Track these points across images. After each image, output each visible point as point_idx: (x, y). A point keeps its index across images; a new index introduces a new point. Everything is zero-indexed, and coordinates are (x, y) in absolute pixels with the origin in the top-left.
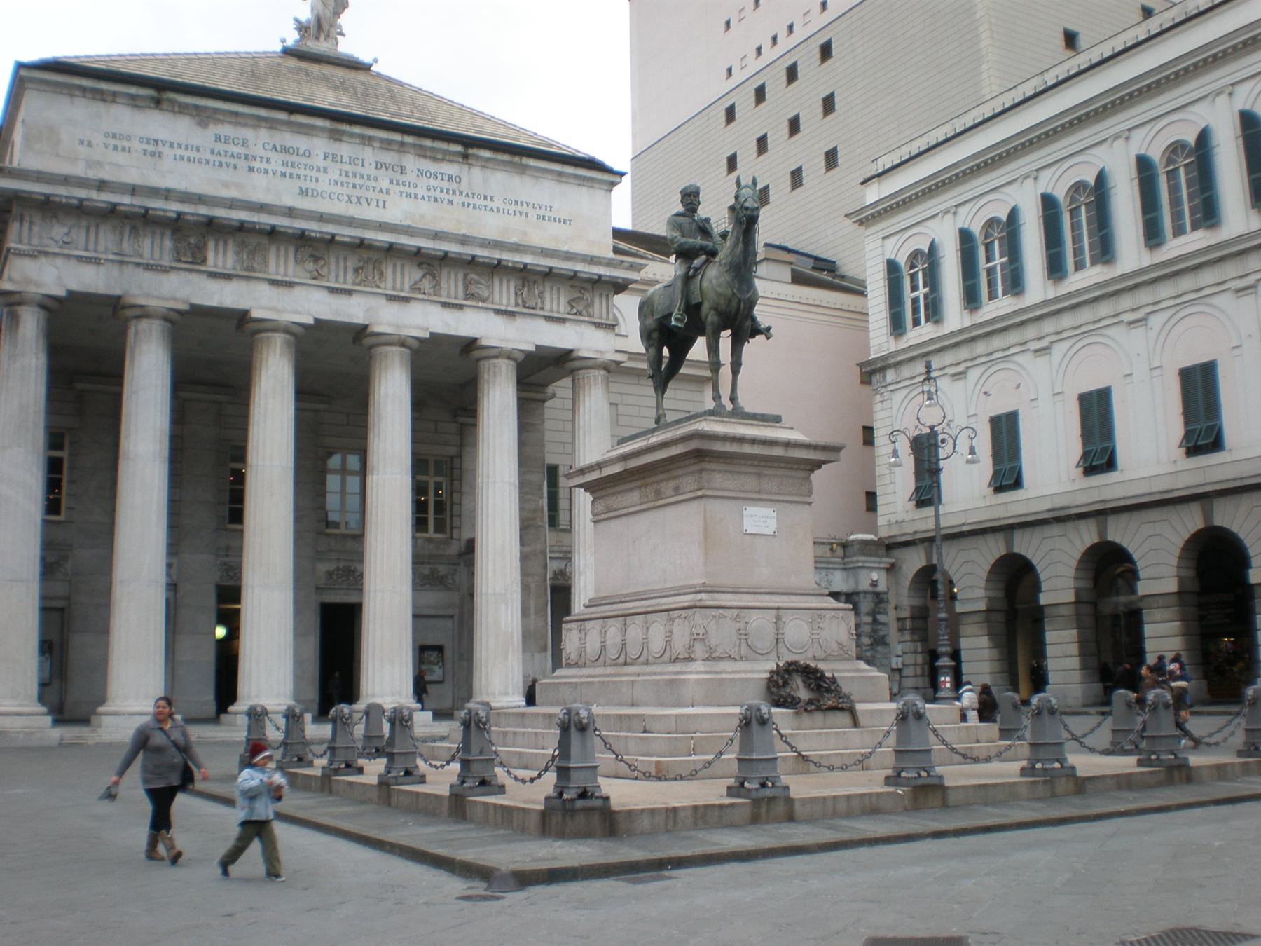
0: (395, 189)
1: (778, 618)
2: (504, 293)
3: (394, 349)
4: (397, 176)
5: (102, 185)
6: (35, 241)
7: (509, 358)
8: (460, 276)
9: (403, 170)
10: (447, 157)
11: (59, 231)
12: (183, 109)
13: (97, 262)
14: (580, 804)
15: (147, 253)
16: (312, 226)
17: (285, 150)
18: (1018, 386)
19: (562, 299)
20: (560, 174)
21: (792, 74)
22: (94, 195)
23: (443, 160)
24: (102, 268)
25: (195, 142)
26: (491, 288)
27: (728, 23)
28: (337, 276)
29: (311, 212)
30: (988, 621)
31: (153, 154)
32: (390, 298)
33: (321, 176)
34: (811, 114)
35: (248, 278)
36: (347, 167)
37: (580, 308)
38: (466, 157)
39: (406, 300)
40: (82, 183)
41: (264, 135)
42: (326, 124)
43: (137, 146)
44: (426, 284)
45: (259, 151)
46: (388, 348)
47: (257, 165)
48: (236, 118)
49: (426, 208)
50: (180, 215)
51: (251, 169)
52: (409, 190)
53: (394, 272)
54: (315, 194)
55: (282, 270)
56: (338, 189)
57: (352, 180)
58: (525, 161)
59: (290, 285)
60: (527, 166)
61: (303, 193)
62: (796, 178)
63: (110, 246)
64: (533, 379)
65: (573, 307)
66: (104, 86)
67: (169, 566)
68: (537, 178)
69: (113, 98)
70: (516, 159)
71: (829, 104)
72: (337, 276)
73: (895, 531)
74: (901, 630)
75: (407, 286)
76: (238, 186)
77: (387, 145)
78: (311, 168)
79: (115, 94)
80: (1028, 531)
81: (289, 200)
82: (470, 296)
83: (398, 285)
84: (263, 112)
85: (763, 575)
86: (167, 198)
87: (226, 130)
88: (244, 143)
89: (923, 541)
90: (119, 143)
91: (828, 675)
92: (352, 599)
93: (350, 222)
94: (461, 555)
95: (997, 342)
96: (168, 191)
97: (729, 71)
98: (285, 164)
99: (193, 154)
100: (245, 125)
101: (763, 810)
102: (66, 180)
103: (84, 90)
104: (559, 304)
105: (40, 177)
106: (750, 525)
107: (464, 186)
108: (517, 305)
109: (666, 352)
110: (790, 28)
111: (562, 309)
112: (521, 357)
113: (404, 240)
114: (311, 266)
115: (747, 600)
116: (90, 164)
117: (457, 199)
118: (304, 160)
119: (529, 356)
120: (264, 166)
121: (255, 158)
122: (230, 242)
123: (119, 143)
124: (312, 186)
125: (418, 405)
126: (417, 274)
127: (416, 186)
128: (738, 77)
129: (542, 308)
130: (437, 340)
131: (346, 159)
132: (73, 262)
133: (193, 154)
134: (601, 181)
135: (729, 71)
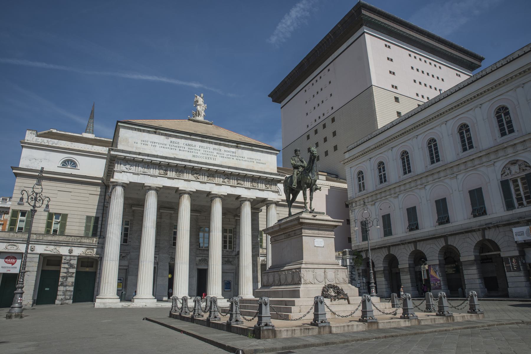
0: (218, 155)
2: (248, 184)
5: (140, 154)
7: (249, 201)
10: (232, 146)
11: (128, 166)
12: (162, 134)
14: (265, 328)
15: (152, 172)
17: (189, 145)
21: (324, 126)
25: (165, 143)
27: (307, 114)
30: (384, 273)
31: (154, 146)
32: (217, 184)
33: (198, 152)
34: (330, 136)
36: (205, 150)
39: (221, 185)
41: (183, 141)
43: (149, 143)
44: (226, 180)
45: (182, 145)
47: (181, 149)
49: (226, 160)
50: (160, 162)
51: (180, 150)
54: (196, 157)
56: (203, 155)
59: (189, 181)
62: (326, 153)
64: (256, 207)
67: (155, 257)
69: (144, 131)
71: (334, 134)
73: (357, 248)
74: (359, 276)
76: (176, 154)
79: (144, 130)
80: (394, 247)
81: (189, 158)
85: (321, 259)
87: (174, 139)
88: (178, 143)
89: (364, 251)
91: (340, 288)
92: (206, 268)
94: (236, 255)
95: (383, 195)
96: (157, 155)
97: (308, 126)
98: (189, 149)
99: (165, 146)
101: (322, 330)
102: (130, 152)
105: (123, 151)
109: (291, 195)
110: (324, 115)
112: (252, 200)
114: (195, 175)
115: (316, 266)
116: (137, 148)
117: (235, 158)
118: (194, 148)
119: (254, 200)
120: (183, 149)
123: (145, 143)
124: (196, 154)
125: (224, 214)
128: (310, 127)
130: (229, 195)
133: (165, 146)
135: (308, 126)
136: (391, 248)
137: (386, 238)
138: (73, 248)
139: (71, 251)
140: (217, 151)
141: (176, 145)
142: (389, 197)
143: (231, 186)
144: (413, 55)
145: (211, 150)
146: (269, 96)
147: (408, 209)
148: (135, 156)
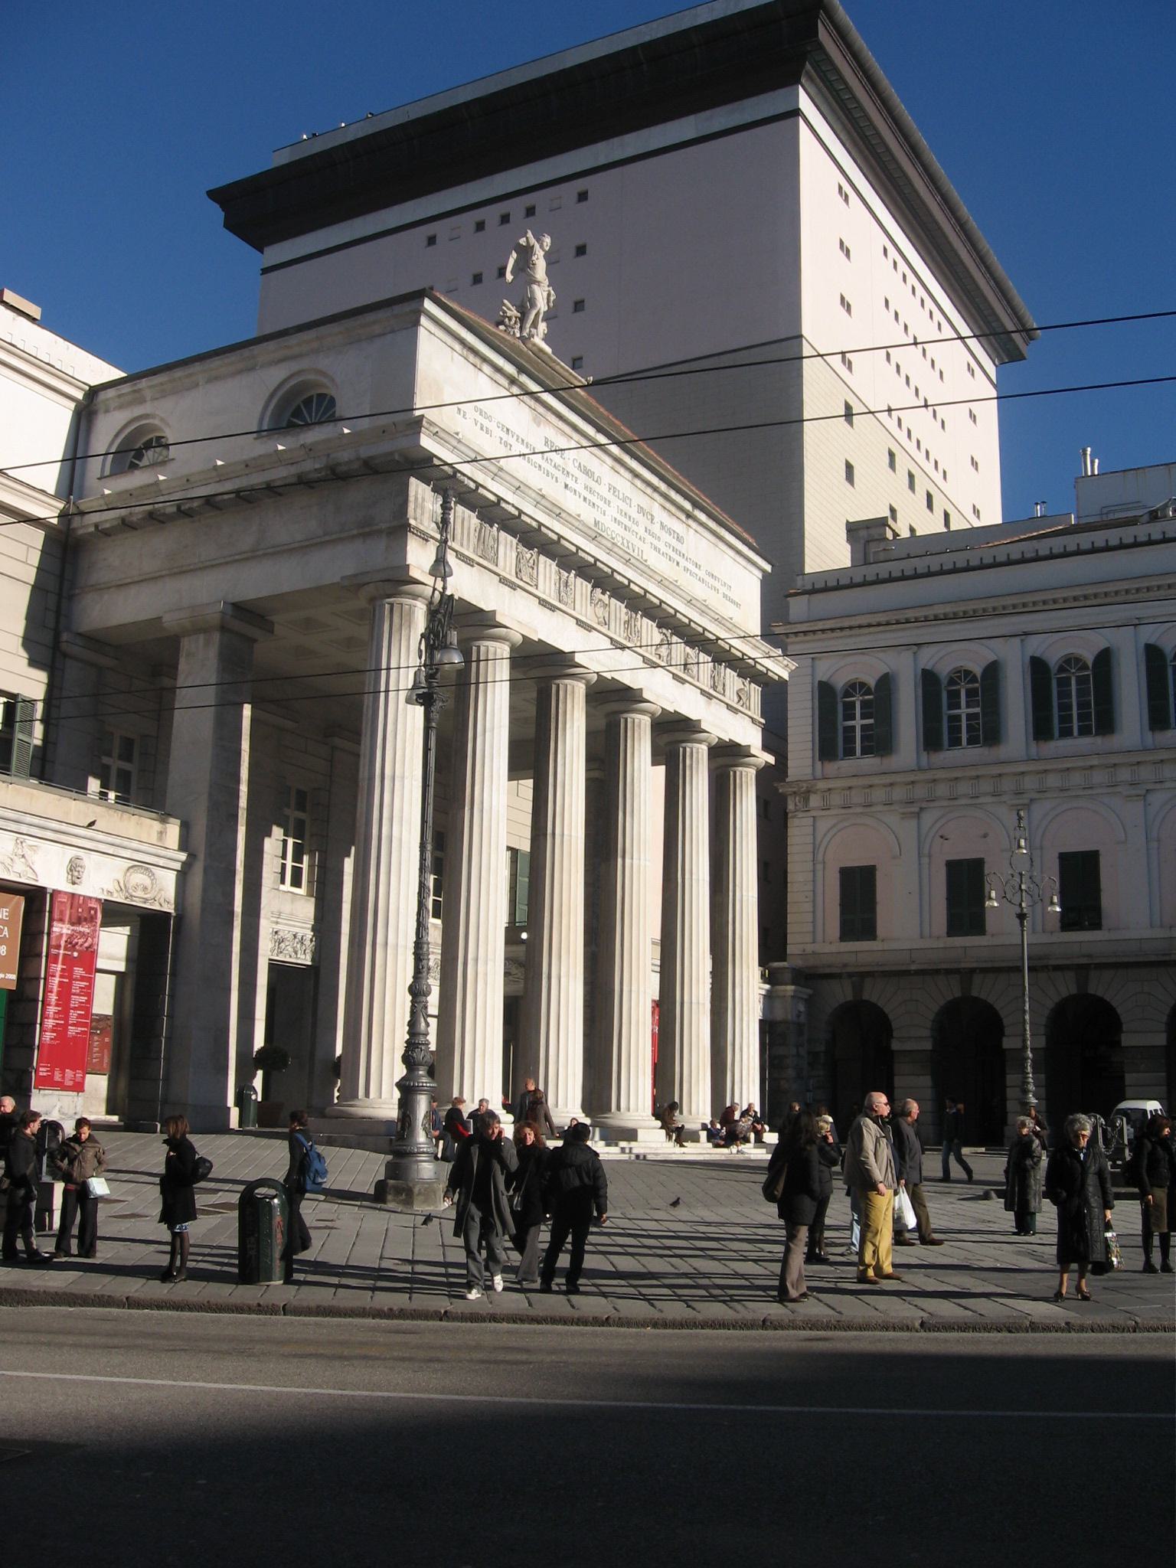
0: (646, 535)
17: (587, 472)
18: (985, 836)
38: (689, 516)
47: (571, 483)
51: (566, 486)
78: (602, 498)
79: (485, 359)
89: (850, 975)
90: (486, 423)
114: (600, 611)
136: (977, 979)
137: (959, 941)
138: (90, 861)
139: (74, 870)
142: (989, 799)
144: (892, 252)
145: (633, 512)
146: (214, 195)
147: (1064, 858)
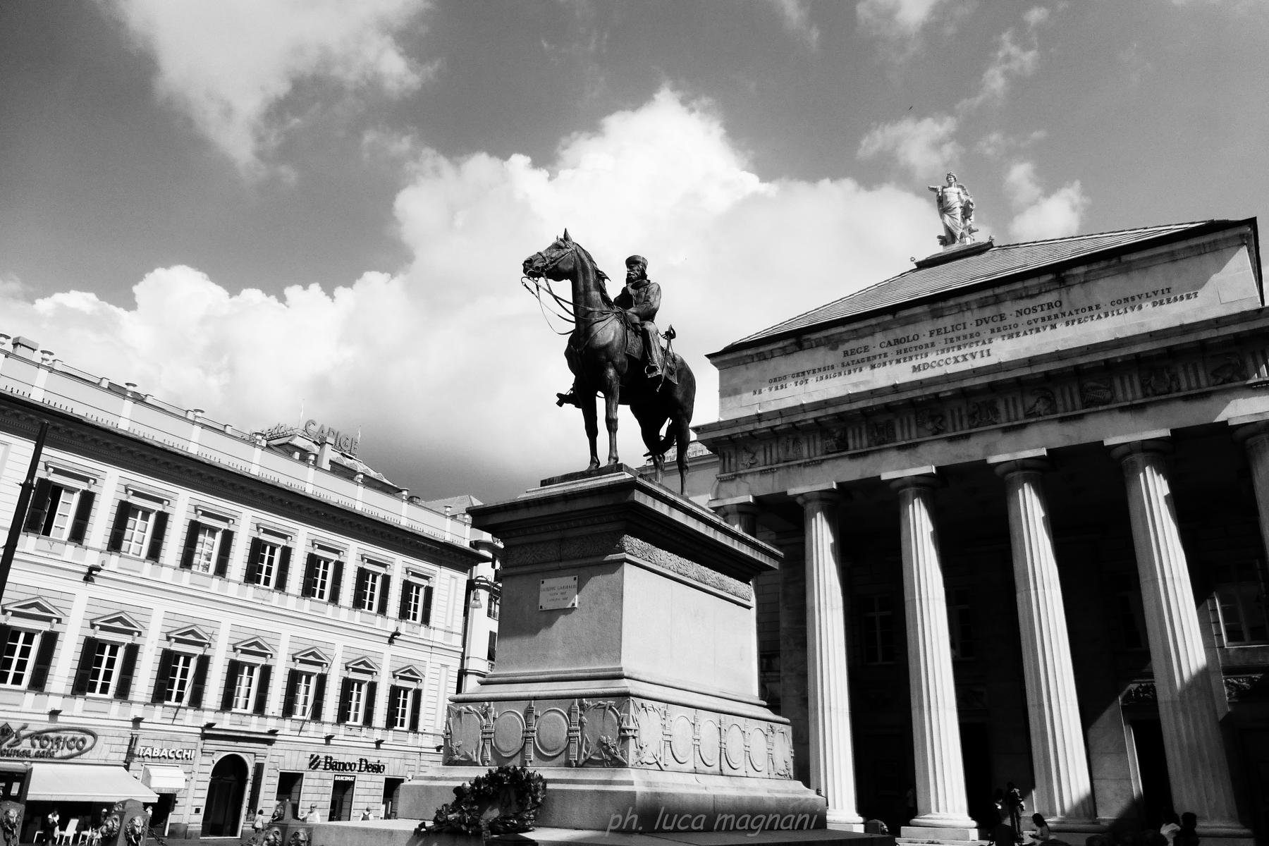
1: (528, 712)
3: (1016, 474)
4: (999, 324)
6: (733, 468)
8: (1075, 389)
9: (1002, 317)
11: (746, 459)
12: (819, 344)
13: (772, 471)
16: (918, 393)
17: (898, 342)
19: (1201, 374)
20: (1172, 254)
22: (758, 426)
23: (1040, 293)
24: (776, 475)
26: (1111, 388)
28: (954, 426)
29: (912, 382)
32: (1006, 430)
35: (880, 451)
37: (1228, 375)
39: (1023, 427)
40: (749, 420)
41: (879, 337)
42: (925, 308)
44: (1040, 407)
45: (878, 351)
46: (1011, 475)
48: (858, 335)
50: (815, 419)
52: (1010, 332)
53: (1007, 407)
54: (926, 366)
55: (906, 436)
57: (956, 344)
58: (1125, 258)
60: (1130, 262)
61: (915, 369)
63: (782, 457)
65: (1217, 377)
66: (762, 349)
68: (1145, 268)
69: (772, 355)
70: (1114, 261)
72: (954, 426)
75: (1021, 414)
77: (983, 305)
78: (921, 347)
79: (771, 351)
82: (1086, 405)
83: (1012, 417)
84: (873, 321)
86: (805, 411)
87: (852, 345)
88: (866, 349)
93: (947, 378)
98: (899, 352)
100: (866, 336)
103: (752, 357)
104: (1198, 380)
106: (546, 602)
107: (1065, 308)
108: (1145, 395)
111: (1203, 383)
113: (1001, 376)
114: (929, 426)
121: (875, 357)
122: (864, 427)
126: (1030, 401)
127: (1016, 326)
129: (1179, 390)
131: (949, 329)
132: (758, 476)
134: (1227, 240)
140: (992, 325)
141: (859, 357)
143: (1062, 420)
145: (971, 329)
148: (750, 427)
